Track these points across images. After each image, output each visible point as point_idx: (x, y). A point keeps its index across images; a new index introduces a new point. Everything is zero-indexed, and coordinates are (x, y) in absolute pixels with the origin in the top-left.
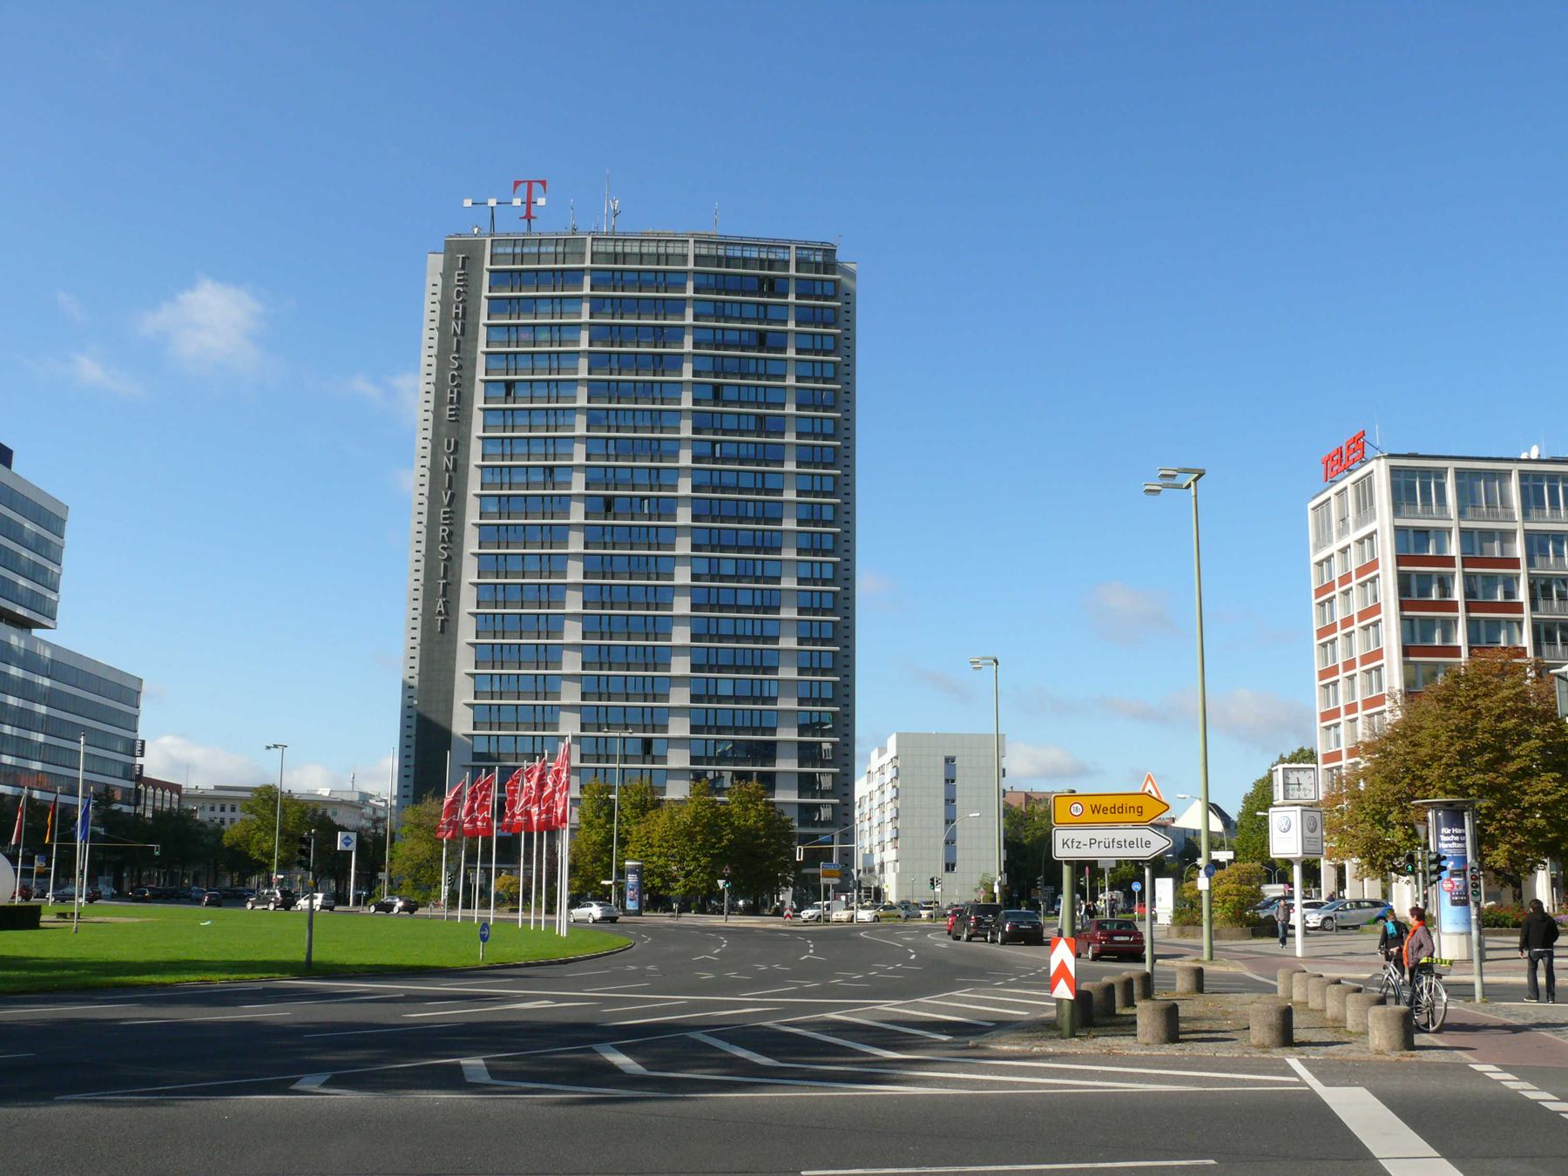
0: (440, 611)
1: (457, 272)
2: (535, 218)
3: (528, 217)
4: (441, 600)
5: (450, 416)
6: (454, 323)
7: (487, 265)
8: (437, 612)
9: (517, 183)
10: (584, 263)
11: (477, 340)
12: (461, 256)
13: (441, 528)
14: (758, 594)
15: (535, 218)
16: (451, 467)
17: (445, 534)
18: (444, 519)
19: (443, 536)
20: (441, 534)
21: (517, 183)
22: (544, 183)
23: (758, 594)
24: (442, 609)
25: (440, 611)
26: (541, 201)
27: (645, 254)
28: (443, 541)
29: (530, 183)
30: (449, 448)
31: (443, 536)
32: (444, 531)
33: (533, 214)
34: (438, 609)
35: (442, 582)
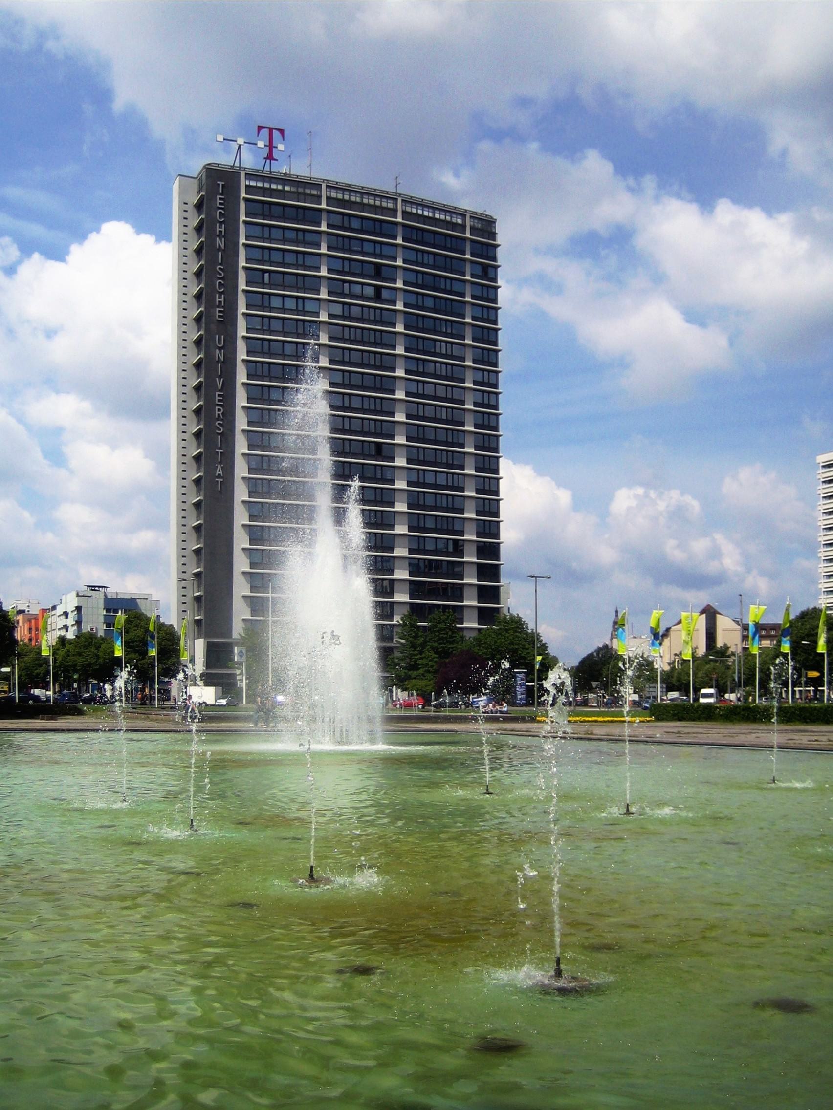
1: (218, 197)
2: (277, 160)
3: (270, 157)
4: (219, 466)
5: (219, 316)
7: (243, 195)
11: (238, 256)
12: (221, 183)
13: (217, 408)
15: (277, 160)
16: (222, 359)
20: (217, 413)
21: (260, 128)
22: (282, 132)
24: (221, 473)
26: (281, 147)
29: (271, 130)
30: (219, 342)
31: (219, 414)
32: (219, 410)
33: (275, 156)
34: (218, 472)
35: (220, 451)
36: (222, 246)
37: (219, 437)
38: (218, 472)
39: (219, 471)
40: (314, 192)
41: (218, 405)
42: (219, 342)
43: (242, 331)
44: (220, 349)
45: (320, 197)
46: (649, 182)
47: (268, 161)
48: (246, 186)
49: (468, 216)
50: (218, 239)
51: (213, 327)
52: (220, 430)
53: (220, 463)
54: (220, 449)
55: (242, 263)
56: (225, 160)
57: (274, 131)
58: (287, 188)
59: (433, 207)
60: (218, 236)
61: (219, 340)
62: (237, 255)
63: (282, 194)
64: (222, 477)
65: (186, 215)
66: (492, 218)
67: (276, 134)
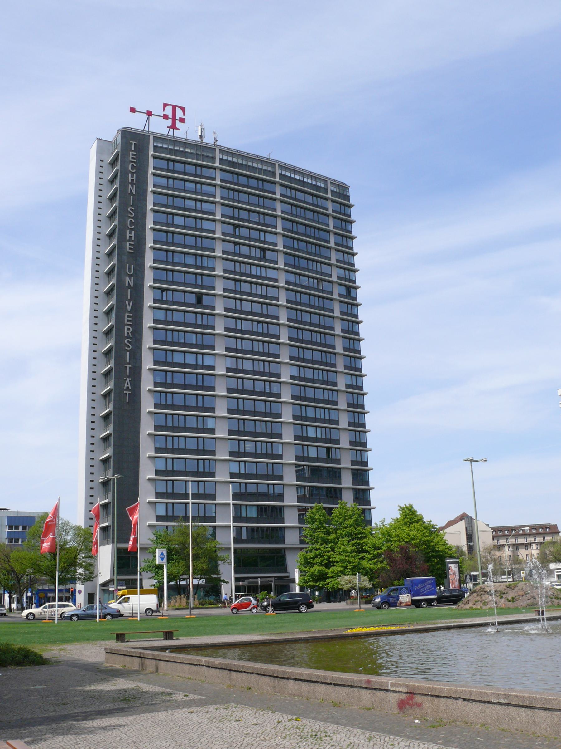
0: (128, 387)
1: (131, 153)
2: (179, 129)
5: (130, 249)
6: (130, 186)
7: (151, 152)
8: (125, 388)
9: (165, 105)
11: (146, 201)
12: (134, 143)
13: (126, 327)
15: (179, 129)
17: (129, 332)
18: (128, 321)
19: (128, 333)
20: (126, 331)
21: (165, 105)
22: (183, 109)
24: (129, 386)
25: (128, 387)
28: (128, 337)
29: (174, 107)
31: (128, 333)
32: (128, 329)
34: (126, 386)
35: (128, 366)
36: (134, 192)
37: (128, 353)
38: (126, 386)
39: (127, 383)
43: (149, 262)
44: (130, 276)
45: (214, 158)
48: (154, 146)
51: (125, 258)
53: (129, 377)
54: (129, 364)
55: (150, 206)
57: (177, 108)
61: (129, 268)
62: (146, 200)
63: (182, 153)
64: (130, 390)
65: (101, 170)
67: (177, 109)
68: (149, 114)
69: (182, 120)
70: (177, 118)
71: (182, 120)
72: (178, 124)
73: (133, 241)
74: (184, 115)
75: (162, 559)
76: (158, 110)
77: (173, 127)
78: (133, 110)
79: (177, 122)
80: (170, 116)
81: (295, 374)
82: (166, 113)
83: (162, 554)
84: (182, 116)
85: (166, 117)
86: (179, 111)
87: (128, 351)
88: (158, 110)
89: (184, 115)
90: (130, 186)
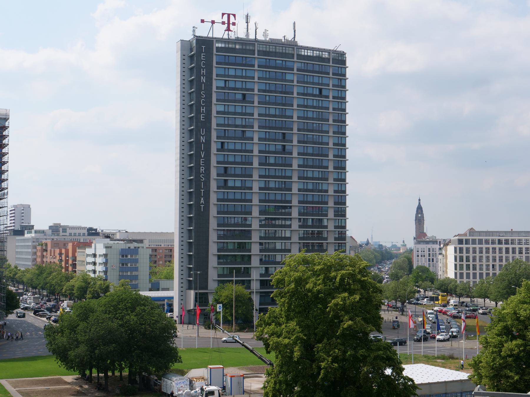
1: (202, 54)
6: (202, 77)
9: (223, 14)
10: (255, 55)
12: (204, 47)
13: (201, 167)
14: (244, 157)
16: (204, 141)
17: (203, 170)
19: (202, 171)
20: (201, 170)
21: (223, 14)
22: (234, 15)
23: (244, 157)
24: (203, 202)
27: (277, 52)
28: (202, 173)
29: (229, 15)
30: (203, 133)
31: (202, 171)
35: (202, 190)
38: (201, 202)
39: (202, 201)
40: (251, 48)
41: (202, 166)
42: (203, 133)
44: (203, 136)
46: (412, 270)
47: (227, 32)
49: (331, 52)
50: (202, 77)
52: (203, 179)
53: (203, 197)
54: (203, 189)
56: (203, 32)
58: (237, 47)
59: (313, 49)
60: (203, 76)
61: (203, 132)
66: (344, 52)
67: (231, 16)
68: (213, 22)
69: (234, 24)
70: (231, 22)
71: (234, 24)
72: (232, 27)
73: (204, 114)
74: (235, 20)
75: (220, 309)
76: (218, 18)
77: (228, 29)
78: (203, 21)
79: (231, 25)
80: (226, 22)
81: (301, 163)
82: (223, 20)
83: (220, 306)
84: (234, 21)
85: (223, 23)
86: (232, 17)
87: (203, 91)
88: (218, 18)
89: (235, 20)
90: (202, 77)
